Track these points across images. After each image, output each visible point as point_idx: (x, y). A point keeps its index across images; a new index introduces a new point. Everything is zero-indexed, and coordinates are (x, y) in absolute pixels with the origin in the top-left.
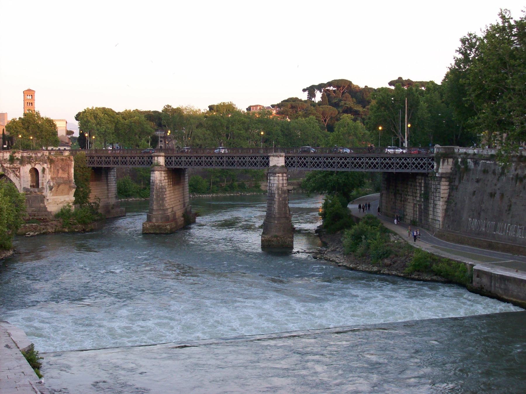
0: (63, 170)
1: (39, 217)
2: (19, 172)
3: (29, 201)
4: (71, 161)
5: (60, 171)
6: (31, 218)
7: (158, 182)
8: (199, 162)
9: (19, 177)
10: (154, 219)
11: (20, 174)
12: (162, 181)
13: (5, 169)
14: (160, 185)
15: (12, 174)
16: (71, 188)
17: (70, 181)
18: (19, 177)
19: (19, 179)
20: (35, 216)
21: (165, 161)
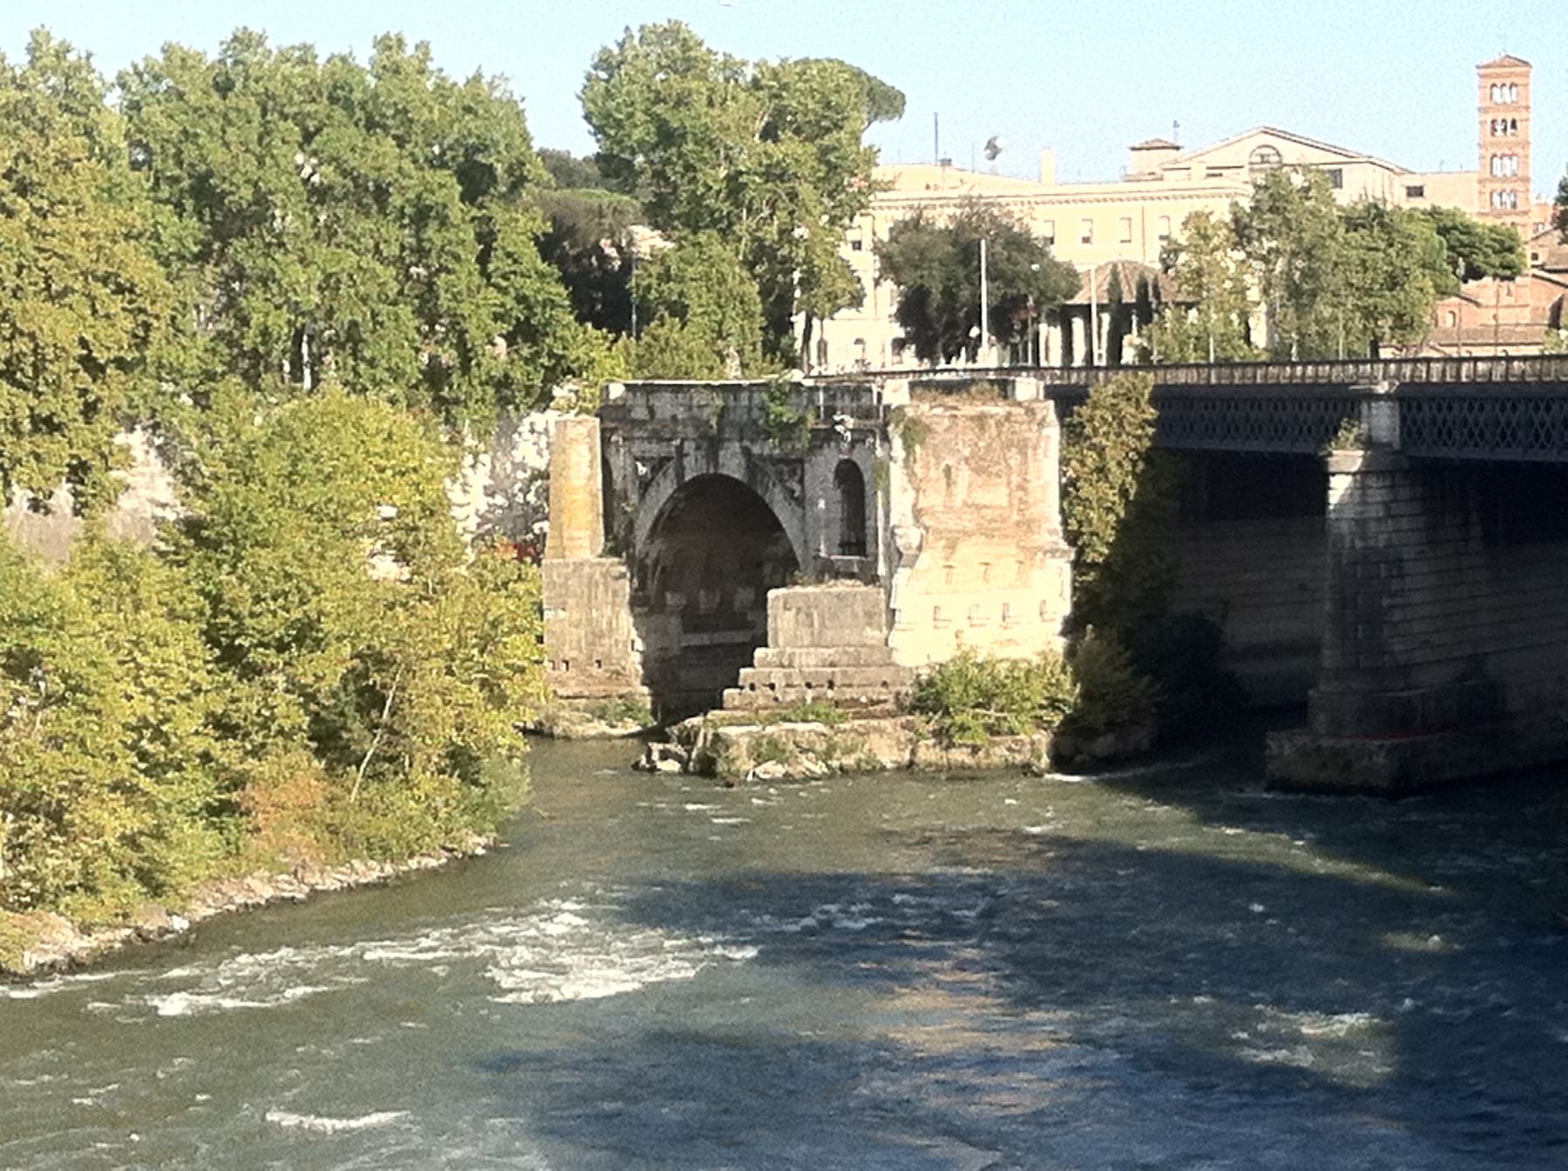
0: (978, 471)
1: (849, 694)
2: (801, 481)
3: (809, 615)
4: (1042, 424)
5: (963, 475)
6: (810, 694)
7: (1345, 528)
8: (1542, 425)
9: (800, 502)
10: (1321, 717)
11: (803, 490)
12: (1372, 526)
13: (755, 466)
14: (1359, 544)
15: (777, 490)
16: (1029, 555)
17: (1028, 525)
18: (800, 502)
19: (799, 511)
20: (831, 685)
21: (1403, 420)
